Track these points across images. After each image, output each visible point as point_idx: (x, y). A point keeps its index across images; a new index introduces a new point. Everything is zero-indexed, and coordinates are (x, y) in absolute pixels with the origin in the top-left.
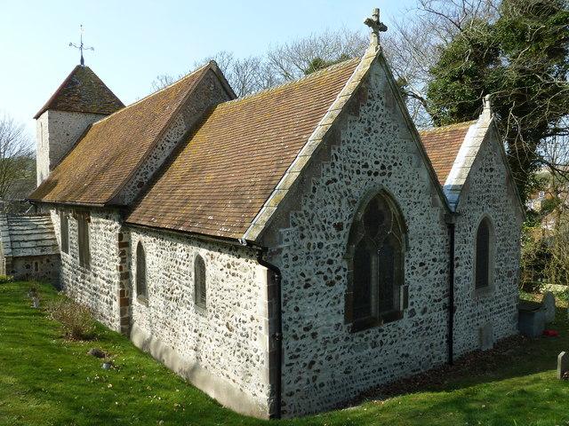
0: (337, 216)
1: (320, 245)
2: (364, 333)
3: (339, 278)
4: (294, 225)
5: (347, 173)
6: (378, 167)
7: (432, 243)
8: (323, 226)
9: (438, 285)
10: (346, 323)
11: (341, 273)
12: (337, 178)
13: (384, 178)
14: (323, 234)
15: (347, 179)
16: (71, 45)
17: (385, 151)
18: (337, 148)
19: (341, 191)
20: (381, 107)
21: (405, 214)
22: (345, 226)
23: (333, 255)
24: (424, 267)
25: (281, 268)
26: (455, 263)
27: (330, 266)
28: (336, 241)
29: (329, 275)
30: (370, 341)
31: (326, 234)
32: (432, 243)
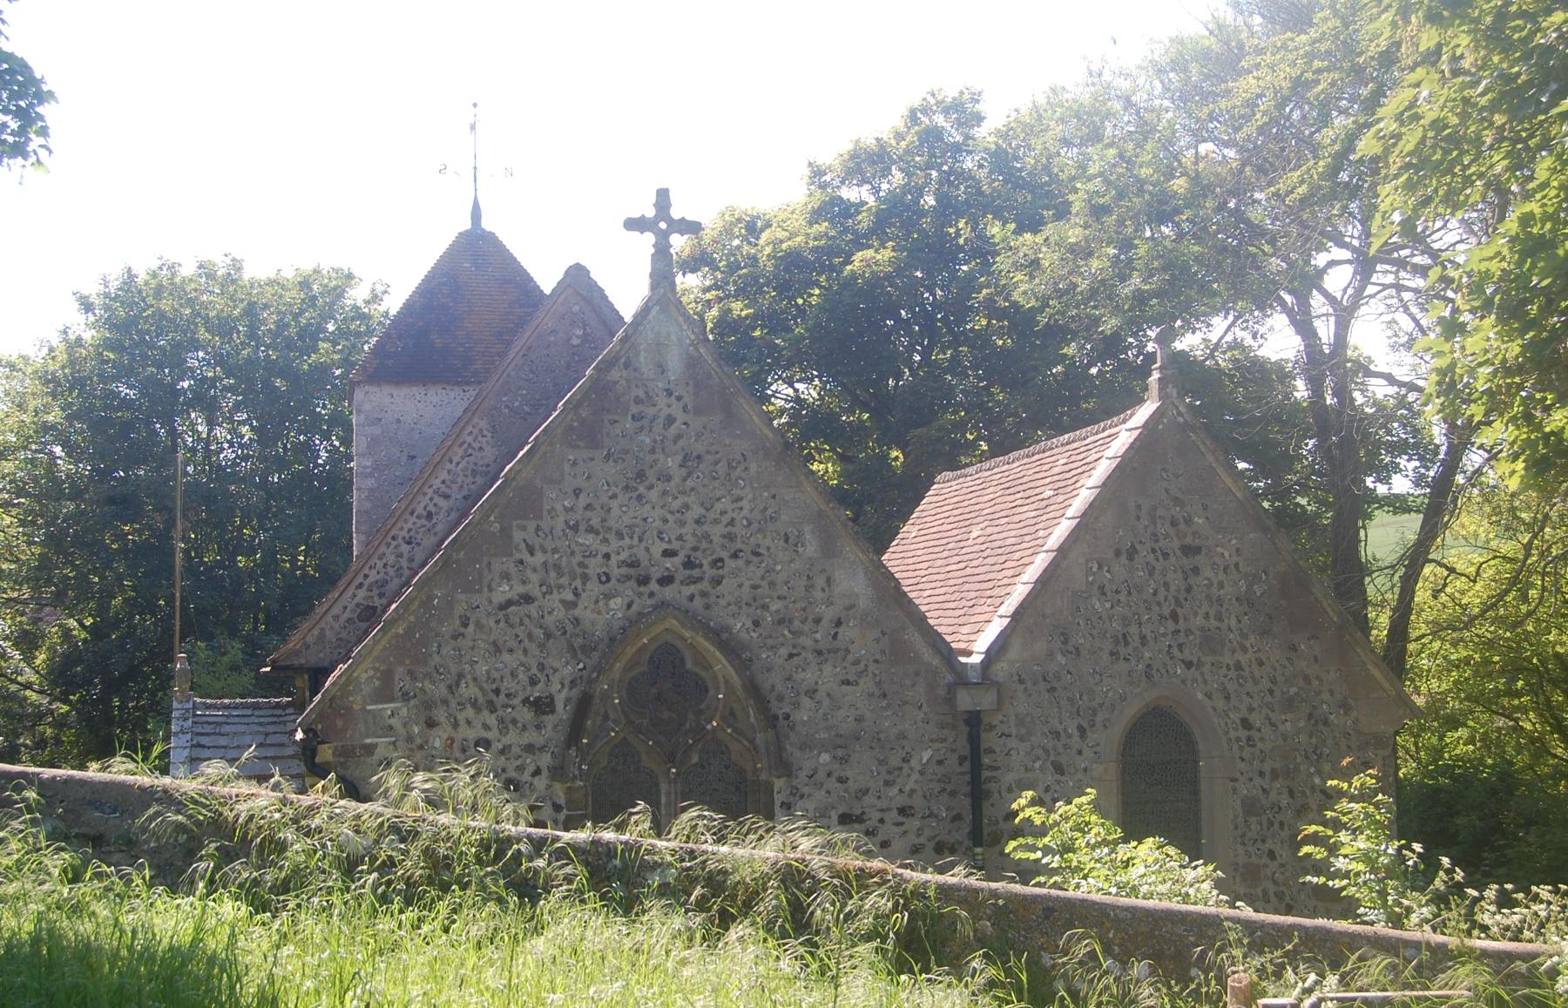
0: (533, 682)
4: (406, 697)
5: (564, 581)
12: (536, 593)
13: (692, 589)
14: (492, 720)
17: (698, 522)
18: (532, 526)
20: (680, 417)
21: (773, 681)
22: (559, 706)
23: (520, 769)
31: (501, 721)
32: (894, 761)
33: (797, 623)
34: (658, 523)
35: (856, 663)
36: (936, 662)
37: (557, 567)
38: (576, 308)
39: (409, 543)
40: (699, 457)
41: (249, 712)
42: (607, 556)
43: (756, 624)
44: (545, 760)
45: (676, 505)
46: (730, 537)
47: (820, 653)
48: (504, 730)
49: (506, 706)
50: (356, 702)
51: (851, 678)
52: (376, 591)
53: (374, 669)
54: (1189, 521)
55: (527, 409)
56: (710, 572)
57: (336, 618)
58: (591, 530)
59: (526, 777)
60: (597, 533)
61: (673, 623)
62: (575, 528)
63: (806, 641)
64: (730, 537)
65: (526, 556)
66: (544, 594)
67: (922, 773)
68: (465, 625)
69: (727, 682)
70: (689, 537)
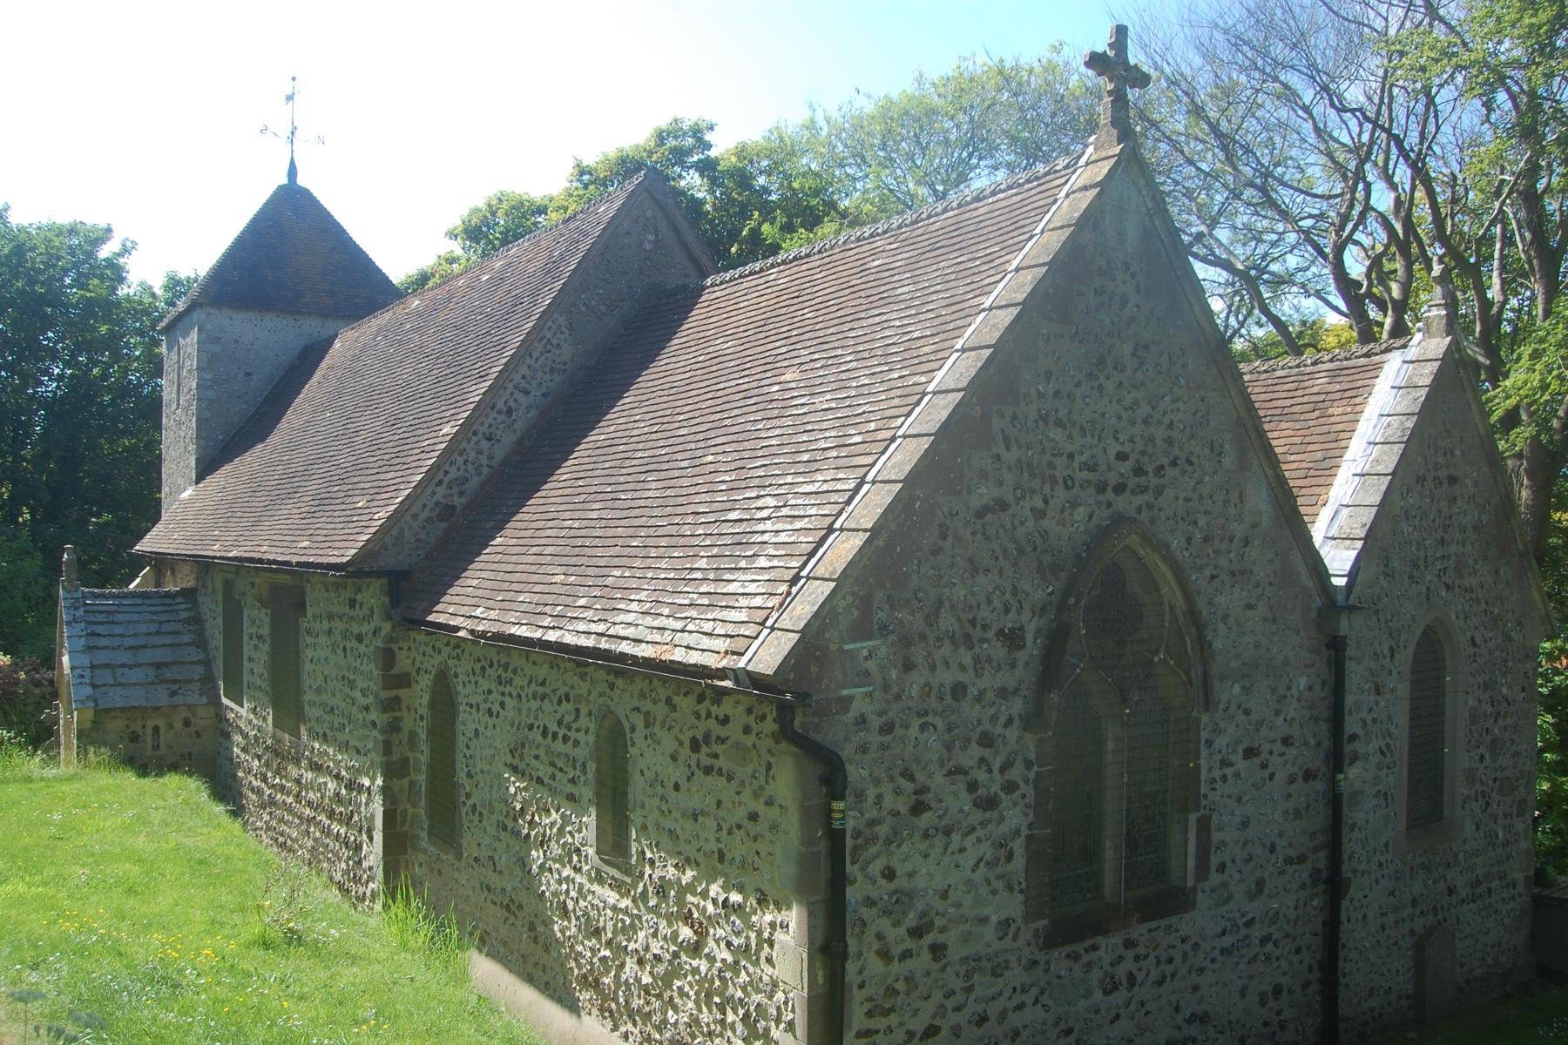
1: (959, 690)
2: (1080, 947)
3: (1010, 787)
4: (884, 630)
5: (1036, 484)
6: (1125, 467)
7: (1282, 690)
8: (968, 637)
9: (1297, 814)
10: (1027, 918)
11: (1016, 773)
12: (1010, 499)
13: (1139, 500)
14: (967, 659)
15: (1039, 504)
16: (264, 130)
17: (1146, 422)
19: (1021, 532)
21: (1201, 603)
23: (994, 719)
24: (1257, 761)
25: (847, 752)
26: (1348, 748)
27: (987, 752)
28: (1007, 679)
29: (981, 776)
30: (1096, 975)
31: (977, 660)
32: (1282, 690)
33: (1217, 541)
34: (1114, 420)
35: (1257, 586)
36: (1310, 584)
37: (1030, 465)
38: (649, 213)
39: (489, 439)
40: (1147, 347)
41: (139, 601)
42: (1071, 456)
43: (1189, 540)
44: (1017, 706)
45: (1128, 400)
46: (1169, 441)
47: (1233, 574)
48: (978, 674)
49: (983, 640)
50: (832, 635)
51: (1252, 601)
52: (456, 489)
53: (853, 594)
54: (1452, 453)
55: (603, 309)
56: (1154, 481)
57: (415, 517)
58: (1059, 424)
59: (999, 729)
60: (1065, 428)
61: (1133, 540)
62: (1045, 419)
63: (1223, 562)
64: (1169, 441)
65: (1000, 449)
66: (1018, 500)
67: (1299, 700)
68: (944, 536)
69: (1172, 608)
70: (1137, 439)
